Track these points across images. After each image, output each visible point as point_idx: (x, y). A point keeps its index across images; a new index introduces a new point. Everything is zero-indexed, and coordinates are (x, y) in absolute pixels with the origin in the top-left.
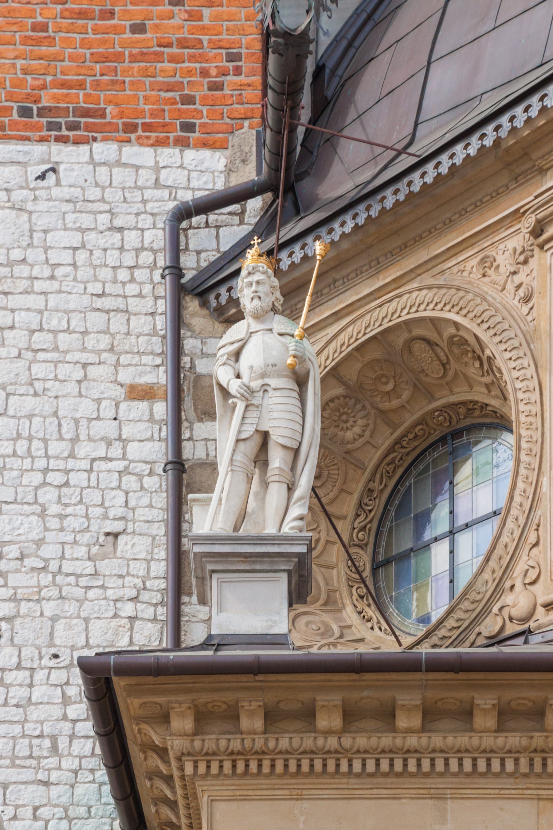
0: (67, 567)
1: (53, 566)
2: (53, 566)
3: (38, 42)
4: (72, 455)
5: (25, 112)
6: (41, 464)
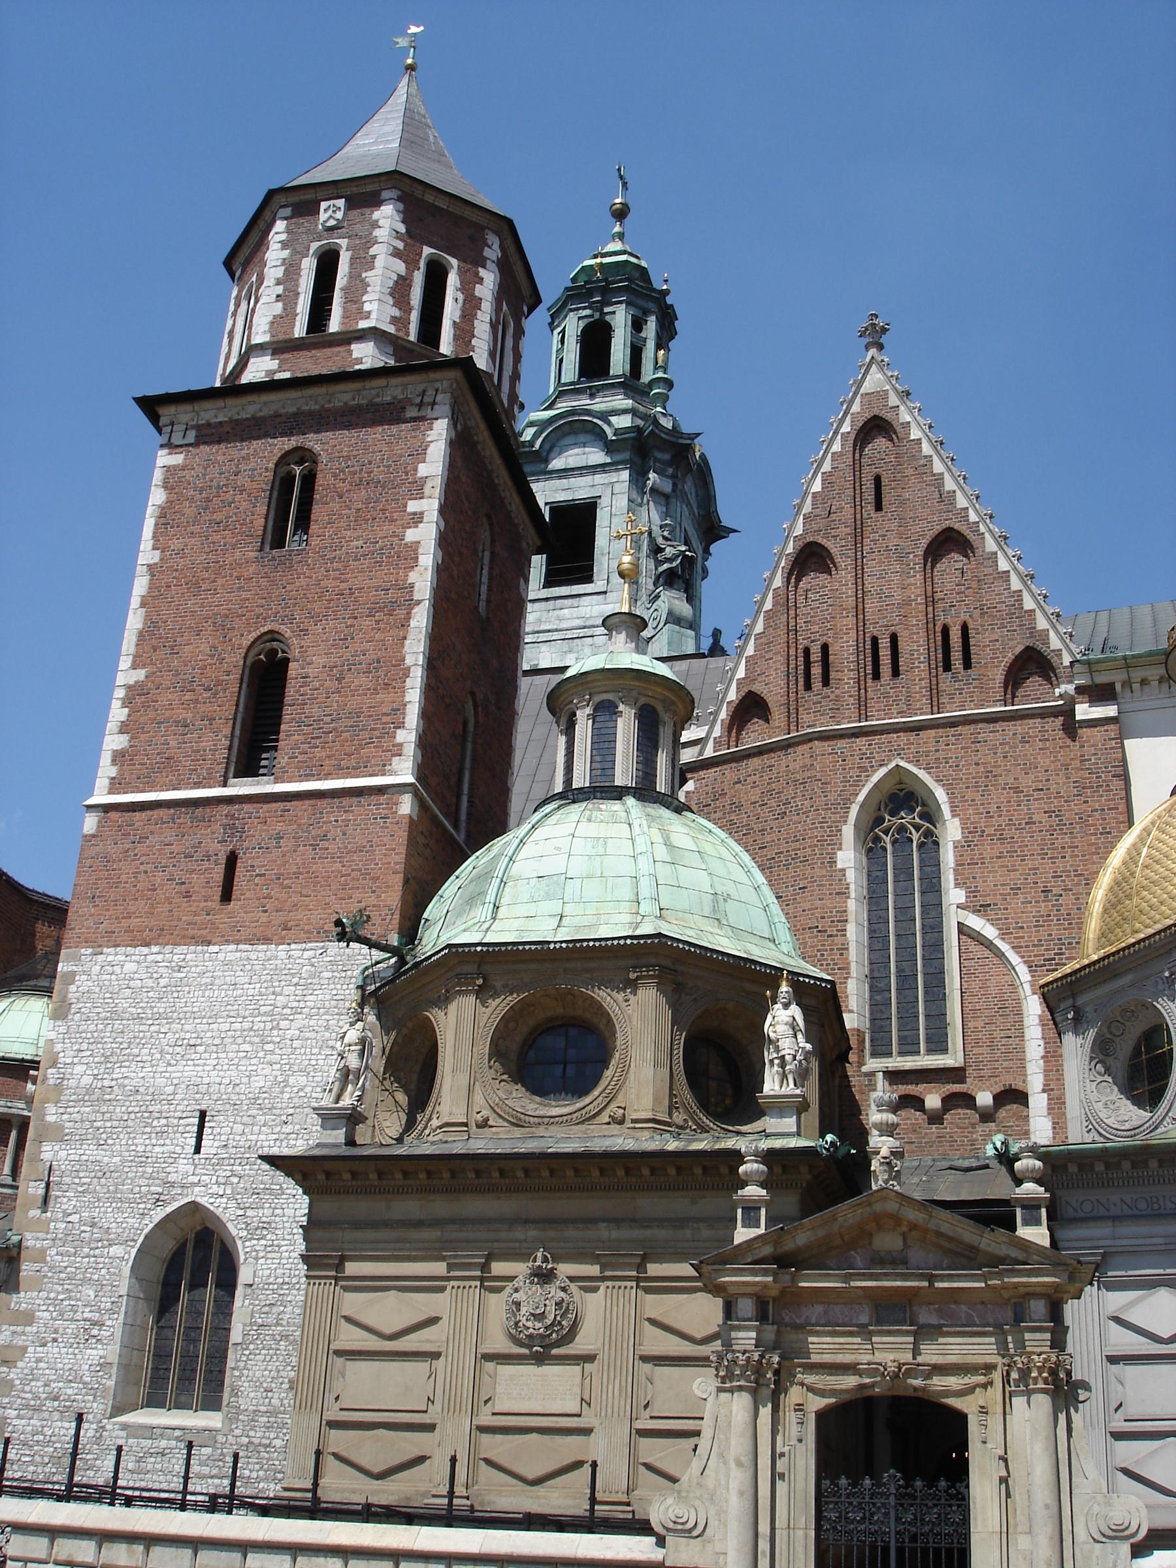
0: (314, 1095)
1: (309, 1095)
2: (309, 1095)
3: (325, 909)
4: (320, 1054)
5: (319, 933)
6: (308, 1057)
